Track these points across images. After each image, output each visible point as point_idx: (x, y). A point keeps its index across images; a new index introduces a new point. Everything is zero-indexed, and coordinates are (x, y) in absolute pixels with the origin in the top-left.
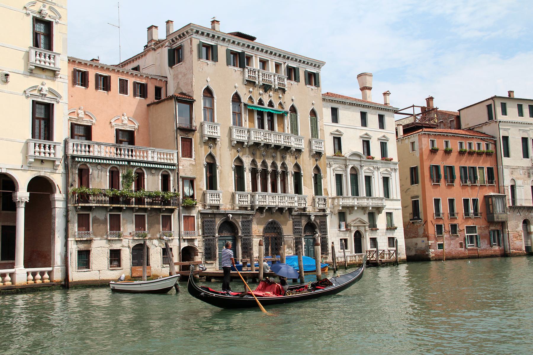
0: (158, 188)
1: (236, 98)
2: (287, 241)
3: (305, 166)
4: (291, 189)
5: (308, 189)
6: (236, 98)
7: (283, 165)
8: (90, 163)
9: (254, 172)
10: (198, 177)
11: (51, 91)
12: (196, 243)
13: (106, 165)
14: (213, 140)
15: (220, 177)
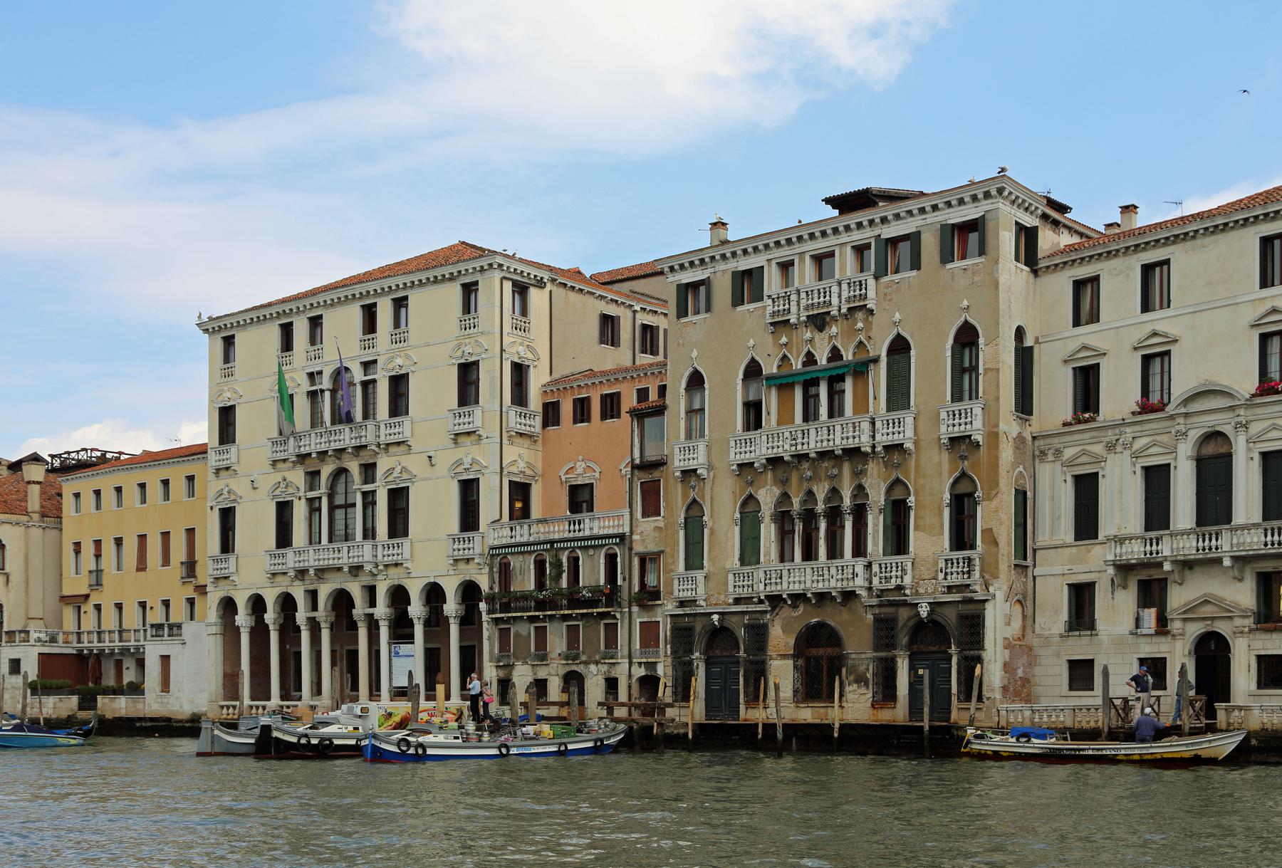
0: (599, 580)
1: (753, 371)
2: (854, 666)
3: (922, 481)
4: (875, 544)
5: (930, 539)
6: (753, 371)
7: (860, 490)
8: (512, 554)
9: (783, 518)
10: (668, 550)
11: (474, 462)
12: (660, 670)
13: (530, 552)
14: (688, 474)
15: (710, 541)
